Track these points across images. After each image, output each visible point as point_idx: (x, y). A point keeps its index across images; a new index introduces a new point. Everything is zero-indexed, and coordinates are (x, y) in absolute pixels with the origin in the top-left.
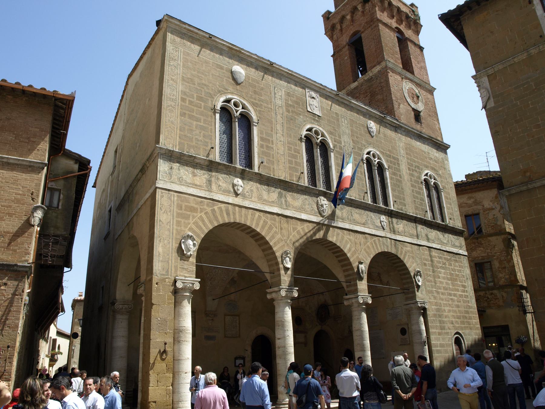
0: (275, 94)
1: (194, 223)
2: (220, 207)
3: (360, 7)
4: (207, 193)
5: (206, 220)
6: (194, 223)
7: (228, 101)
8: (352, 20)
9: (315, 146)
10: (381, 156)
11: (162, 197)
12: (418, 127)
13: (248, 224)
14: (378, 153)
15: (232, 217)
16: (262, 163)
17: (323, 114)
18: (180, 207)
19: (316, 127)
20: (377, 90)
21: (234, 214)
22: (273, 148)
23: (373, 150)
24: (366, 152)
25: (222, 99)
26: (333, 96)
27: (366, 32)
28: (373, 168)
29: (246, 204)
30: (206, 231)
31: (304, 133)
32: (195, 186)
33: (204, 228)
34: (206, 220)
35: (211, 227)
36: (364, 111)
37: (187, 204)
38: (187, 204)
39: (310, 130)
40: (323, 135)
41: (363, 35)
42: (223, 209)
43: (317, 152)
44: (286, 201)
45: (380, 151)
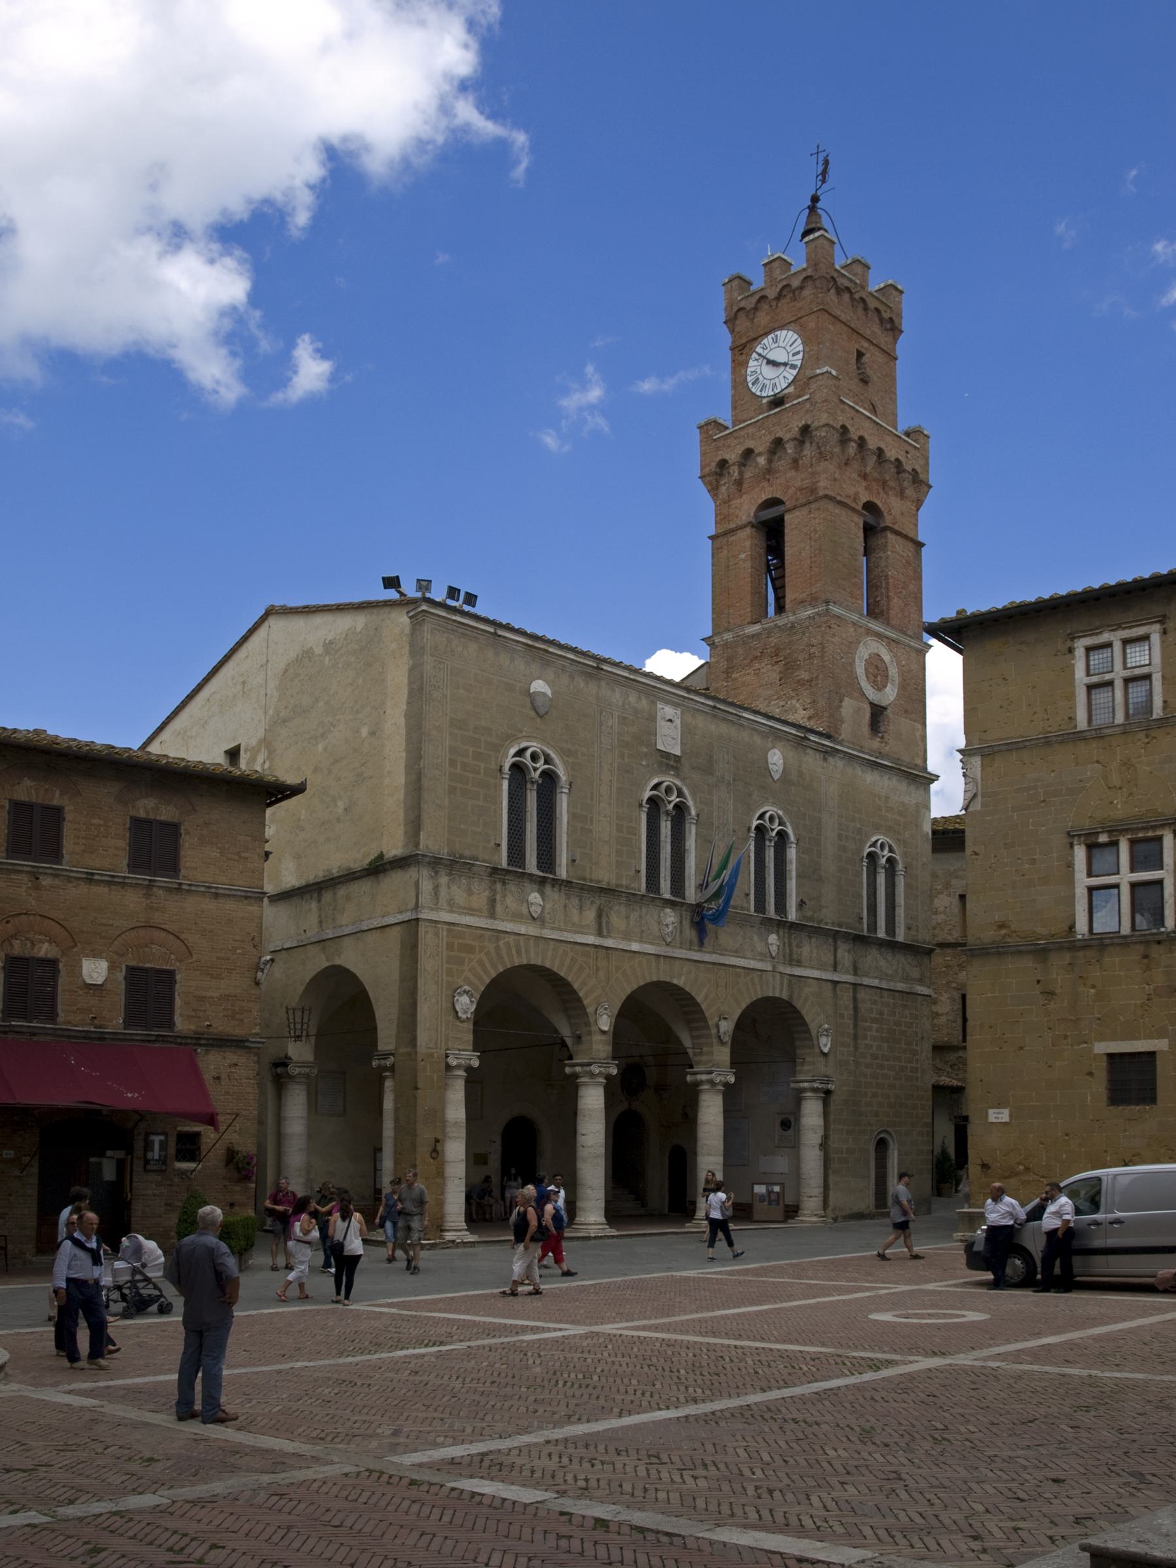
0: (601, 725)
1: (470, 970)
2: (508, 943)
3: (790, 449)
4: (489, 921)
5: (488, 965)
6: (470, 970)
7: (521, 753)
8: (769, 471)
9: (663, 817)
10: (785, 819)
11: (427, 932)
12: (876, 744)
13: (548, 965)
14: (780, 813)
15: (524, 955)
16: (574, 861)
17: (682, 751)
18: (450, 947)
19: (669, 780)
20: (801, 657)
21: (527, 951)
22: (591, 831)
23: (771, 810)
24: (757, 815)
25: (513, 751)
26: (707, 709)
27: (797, 513)
28: (767, 843)
29: (547, 933)
30: (488, 981)
31: (647, 794)
32: (471, 911)
33: (485, 977)
34: (488, 965)
35: (494, 974)
36: (766, 729)
37: (460, 941)
38: (460, 941)
39: (656, 787)
40: (680, 794)
41: (787, 517)
42: (512, 944)
43: (666, 828)
44: (607, 923)
45: (785, 811)
